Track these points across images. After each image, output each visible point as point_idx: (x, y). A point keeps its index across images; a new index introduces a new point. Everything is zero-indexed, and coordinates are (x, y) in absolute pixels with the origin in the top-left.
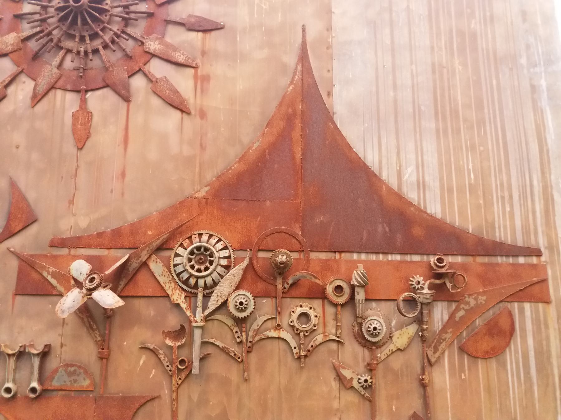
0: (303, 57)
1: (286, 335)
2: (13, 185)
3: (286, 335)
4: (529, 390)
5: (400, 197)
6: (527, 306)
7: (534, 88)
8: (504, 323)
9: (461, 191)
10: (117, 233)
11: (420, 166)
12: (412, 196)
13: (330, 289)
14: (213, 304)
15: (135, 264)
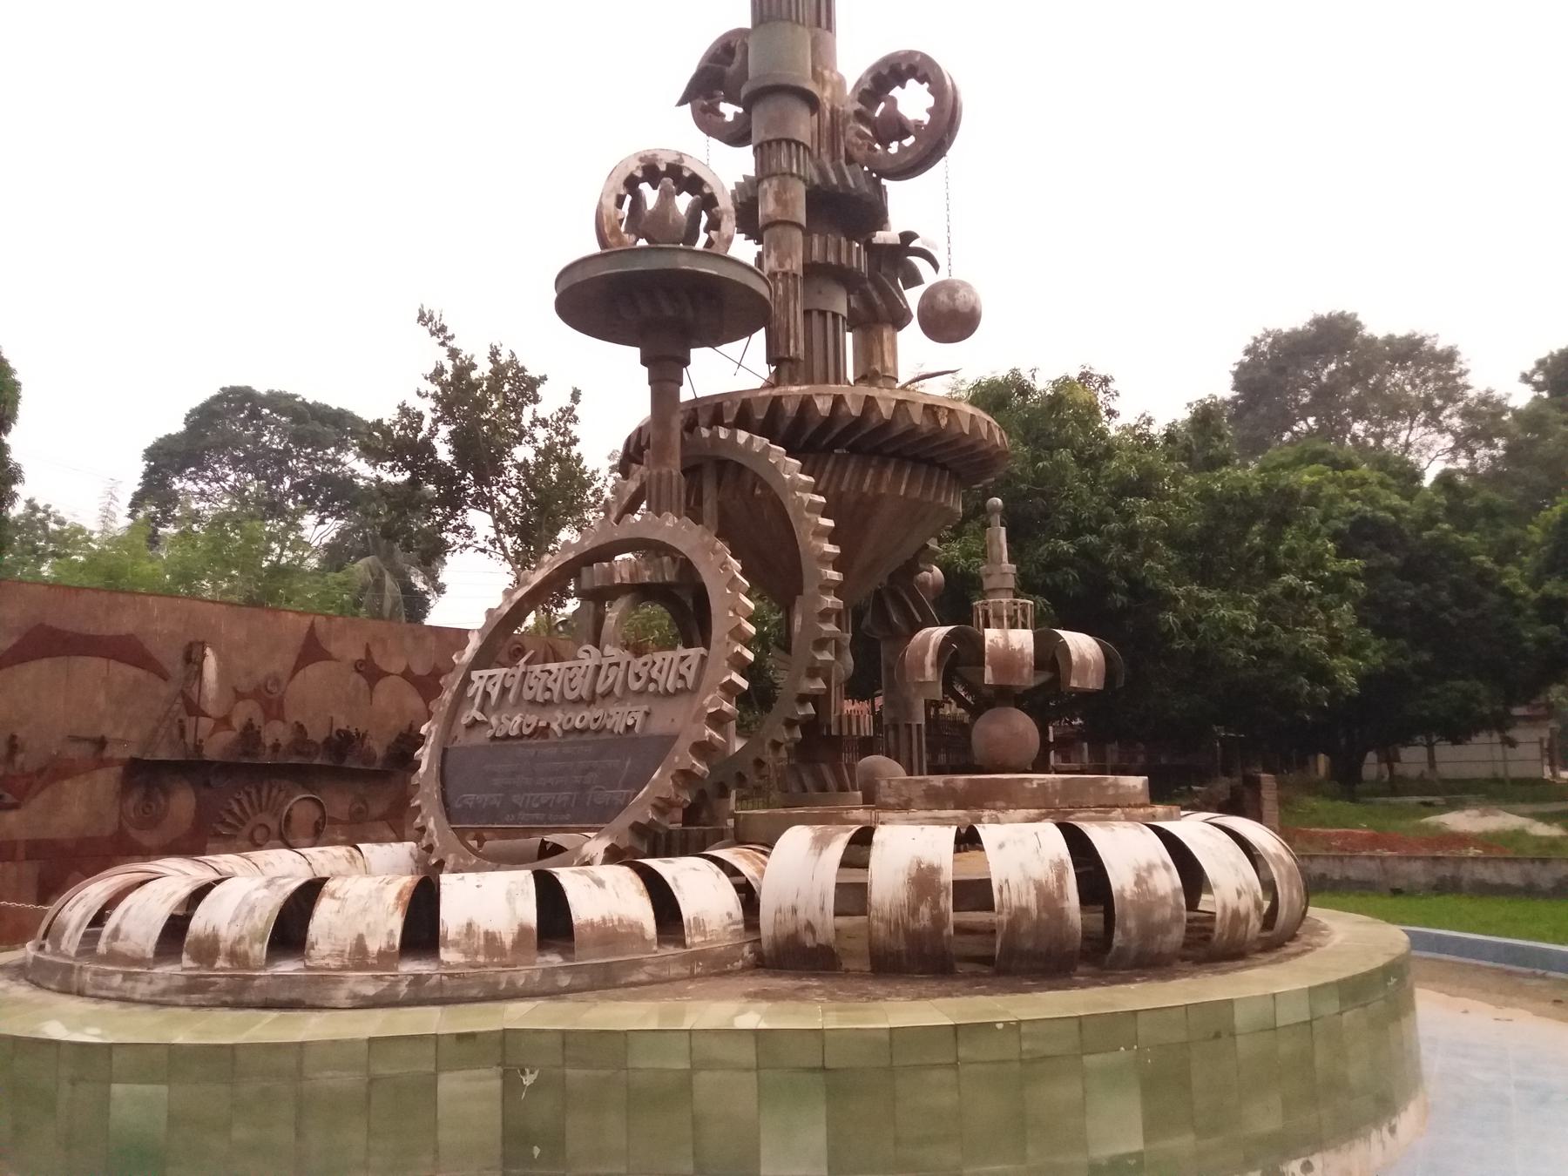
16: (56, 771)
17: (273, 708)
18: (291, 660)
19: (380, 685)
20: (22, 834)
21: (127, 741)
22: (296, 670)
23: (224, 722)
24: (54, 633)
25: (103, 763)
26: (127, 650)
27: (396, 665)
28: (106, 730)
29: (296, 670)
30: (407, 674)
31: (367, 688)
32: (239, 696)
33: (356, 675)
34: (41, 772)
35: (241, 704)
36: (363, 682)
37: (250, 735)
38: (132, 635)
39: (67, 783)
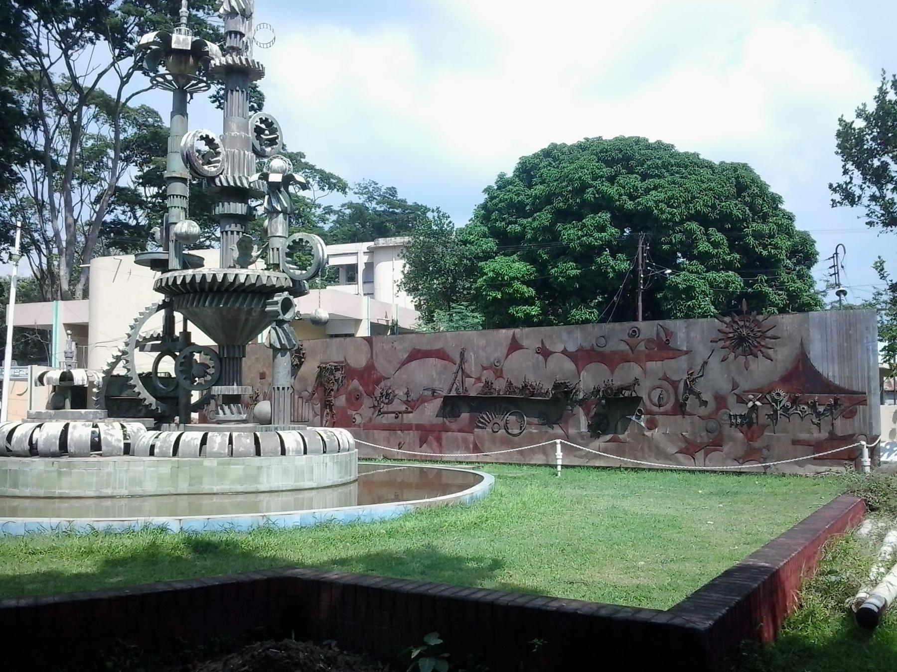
0: (802, 344)
1: (799, 412)
2: (733, 378)
3: (800, 412)
4: (860, 425)
5: (827, 379)
6: (861, 406)
7: (868, 349)
8: (855, 410)
9: (844, 378)
10: (758, 389)
11: (833, 372)
12: (831, 379)
13: (809, 403)
14: (781, 406)
15: (763, 396)
16: (422, 400)
17: (499, 373)
18: (505, 351)
19: (550, 359)
20: (414, 422)
21: (444, 388)
22: (508, 355)
23: (479, 379)
24: (419, 351)
25: (436, 397)
26: (441, 355)
27: (560, 347)
28: (436, 385)
29: (508, 355)
30: (565, 352)
31: (544, 360)
32: (484, 368)
33: (537, 355)
34: (418, 400)
35: (485, 371)
36: (541, 357)
37: (488, 385)
38: (442, 348)
39: (426, 404)
